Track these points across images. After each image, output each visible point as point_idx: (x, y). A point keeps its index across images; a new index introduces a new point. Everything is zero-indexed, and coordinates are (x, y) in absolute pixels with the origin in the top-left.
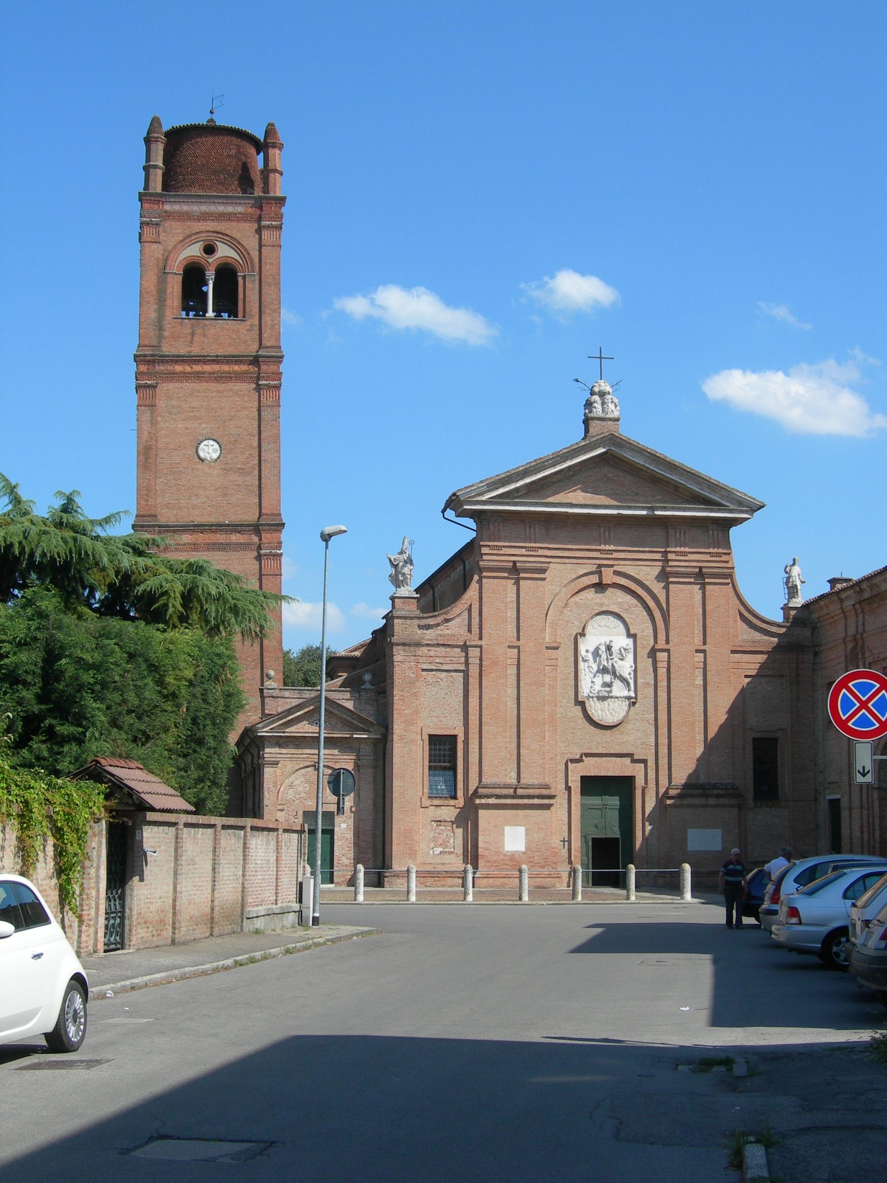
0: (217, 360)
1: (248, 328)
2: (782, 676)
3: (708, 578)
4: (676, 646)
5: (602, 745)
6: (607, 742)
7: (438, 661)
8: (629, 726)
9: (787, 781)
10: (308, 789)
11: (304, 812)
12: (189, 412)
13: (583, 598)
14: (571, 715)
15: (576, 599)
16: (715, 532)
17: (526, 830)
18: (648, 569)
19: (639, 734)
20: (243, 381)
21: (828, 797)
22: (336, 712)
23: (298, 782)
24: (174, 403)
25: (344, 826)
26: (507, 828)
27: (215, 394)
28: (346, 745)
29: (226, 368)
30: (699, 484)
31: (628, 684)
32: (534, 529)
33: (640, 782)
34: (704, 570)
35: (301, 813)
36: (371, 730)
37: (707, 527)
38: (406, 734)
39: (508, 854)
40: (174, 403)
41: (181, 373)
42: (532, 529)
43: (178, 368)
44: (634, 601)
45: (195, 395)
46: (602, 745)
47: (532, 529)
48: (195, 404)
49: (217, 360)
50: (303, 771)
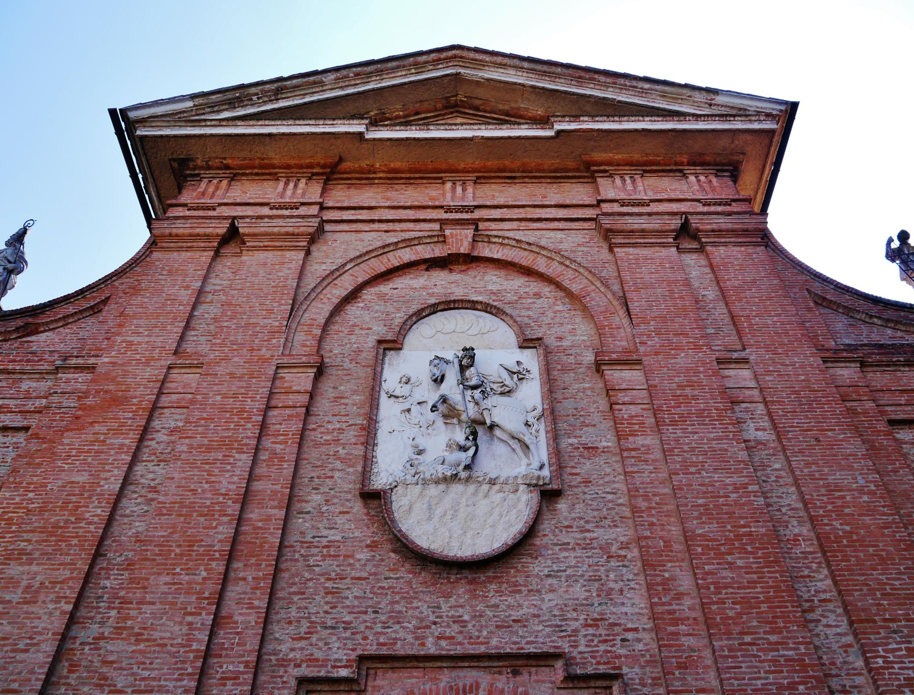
3: (708, 237)
4: (657, 354)
5: (437, 630)
6: (458, 620)
8: (538, 567)
13: (399, 286)
14: (335, 536)
15: (384, 288)
16: (702, 178)
18: (560, 235)
19: (578, 591)
30: (643, 92)
31: (526, 447)
32: (296, 186)
34: (693, 220)
37: (681, 171)
42: (291, 185)
44: (534, 286)
46: (437, 630)
47: (291, 185)
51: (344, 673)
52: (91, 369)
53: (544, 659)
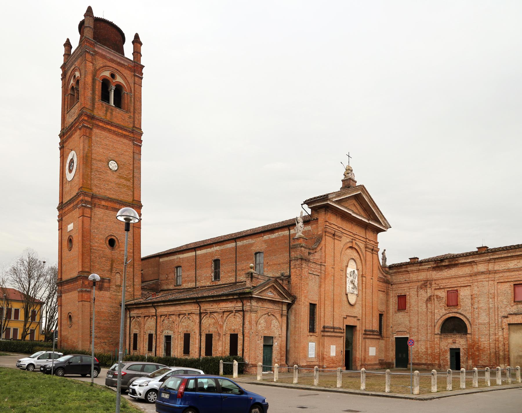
0: (117, 126)
1: (129, 117)
2: (384, 292)
7: (313, 270)
8: (356, 306)
9: (385, 330)
10: (265, 325)
11: (264, 336)
12: (105, 145)
17: (336, 347)
20: (127, 139)
21: (395, 337)
22: (278, 289)
23: (262, 322)
24: (98, 139)
25: (276, 344)
26: (331, 346)
27: (115, 141)
28: (278, 305)
29: (120, 131)
33: (358, 328)
35: (263, 337)
36: (289, 299)
38: (304, 302)
39: (331, 357)
40: (98, 139)
41: (101, 126)
43: (101, 124)
45: (107, 138)
48: (107, 143)
49: (117, 126)
50: (264, 316)
51: (345, 317)
52: (325, 266)
53: (356, 317)
